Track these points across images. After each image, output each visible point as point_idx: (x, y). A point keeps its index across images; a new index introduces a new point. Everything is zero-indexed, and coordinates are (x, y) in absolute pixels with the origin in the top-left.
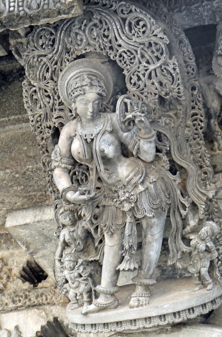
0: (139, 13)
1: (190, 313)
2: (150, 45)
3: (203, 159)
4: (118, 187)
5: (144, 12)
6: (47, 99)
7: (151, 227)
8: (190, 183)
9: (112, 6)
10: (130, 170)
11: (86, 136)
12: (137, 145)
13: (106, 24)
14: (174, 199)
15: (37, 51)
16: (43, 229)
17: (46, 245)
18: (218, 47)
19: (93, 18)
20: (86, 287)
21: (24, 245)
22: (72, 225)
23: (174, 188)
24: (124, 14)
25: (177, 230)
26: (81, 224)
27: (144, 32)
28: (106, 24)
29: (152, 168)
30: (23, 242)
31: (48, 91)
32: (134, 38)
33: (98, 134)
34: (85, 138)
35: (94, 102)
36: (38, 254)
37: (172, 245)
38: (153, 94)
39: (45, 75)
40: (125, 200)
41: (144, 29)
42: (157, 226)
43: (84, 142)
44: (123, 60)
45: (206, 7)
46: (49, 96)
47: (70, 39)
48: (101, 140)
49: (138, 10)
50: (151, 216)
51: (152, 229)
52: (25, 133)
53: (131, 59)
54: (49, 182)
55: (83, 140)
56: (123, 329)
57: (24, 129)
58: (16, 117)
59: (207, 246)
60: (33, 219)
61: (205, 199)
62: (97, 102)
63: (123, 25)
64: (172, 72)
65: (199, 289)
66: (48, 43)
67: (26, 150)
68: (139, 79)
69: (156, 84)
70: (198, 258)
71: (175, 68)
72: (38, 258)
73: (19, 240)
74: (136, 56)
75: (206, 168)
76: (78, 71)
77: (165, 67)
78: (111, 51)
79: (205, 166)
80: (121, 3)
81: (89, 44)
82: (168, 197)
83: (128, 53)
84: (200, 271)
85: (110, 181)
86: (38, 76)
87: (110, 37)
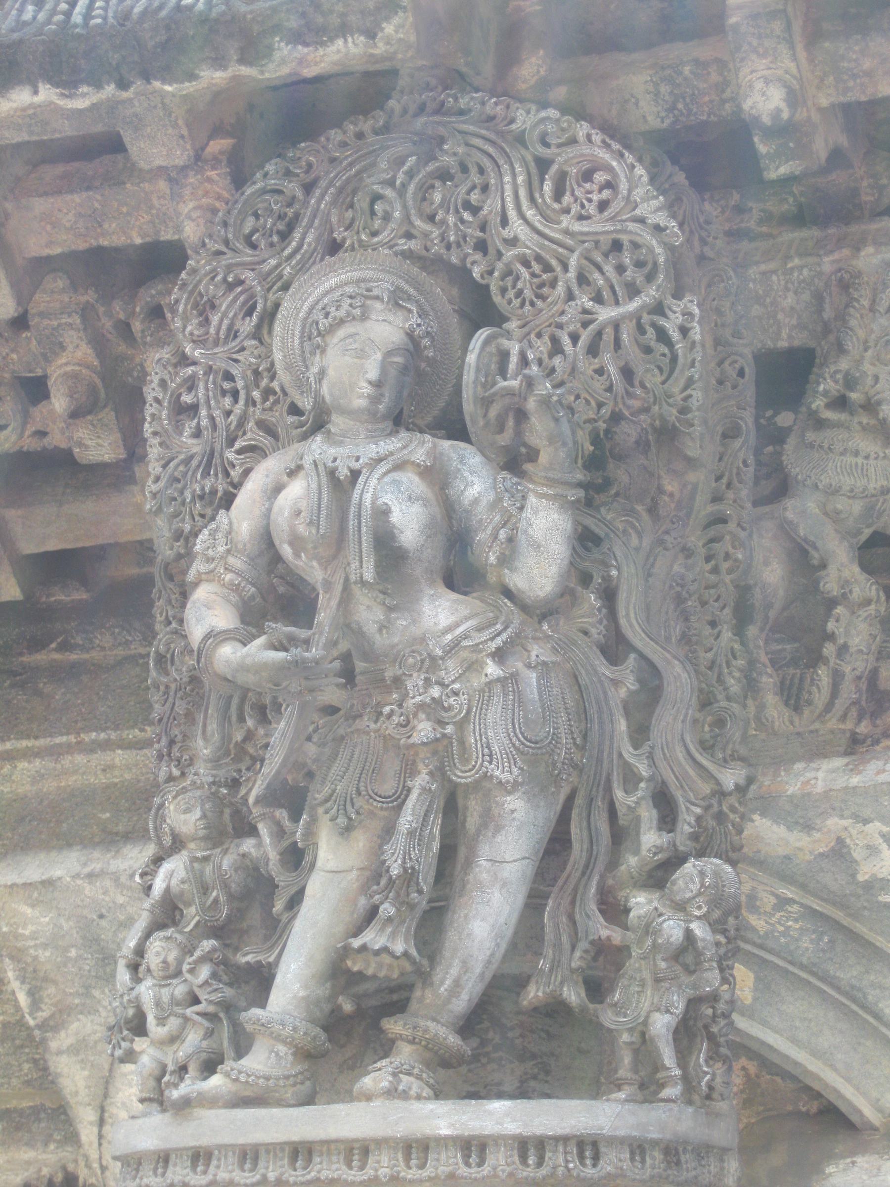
0: (599, 147)
1: (581, 1157)
2: (617, 246)
3: (720, 674)
4: (411, 660)
5: (616, 146)
6: (227, 401)
7: (498, 829)
8: (663, 723)
9: (512, 121)
10: (466, 612)
11: (335, 460)
12: (509, 526)
13: (481, 171)
14: (601, 752)
15: (230, 254)
16: (101, 916)
17: (96, 993)
18: (819, 384)
19: (441, 150)
20: (205, 1044)
21: (23, 982)
22: (205, 838)
23: (610, 708)
24: (547, 145)
25: (587, 866)
26: (238, 846)
27: (603, 206)
28: (481, 171)
29: (543, 632)
30: (24, 970)
31: (235, 372)
32: (565, 221)
33: (380, 460)
34: (330, 464)
35: (389, 354)
36: (63, 1034)
37: (557, 926)
38: (593, 403)
39: (238, 325)
40: (421, 706)
41: (606, 194)
42: (519, 828)
43: (324, 479)
44: (514, 287)
45: (796, 274)
46: (235, 394)
47: (349, 214)
48: (386, 479)
49: (597, 137)
50: (505, 777)
51: (499, 838)
52: (116, 784)
53: (541, 285)
54: (160, 720)
55: (323, 474)
56: (313, 1174)
57: (116, 773)
58: (103, 735)
59: (689, 935)
60: (76, 868)
61: (706, 788)
62: (398, 359)
63: (536, 183)
64: (675, 335)
65: (626, 1101)
66: (274, 224)
67: (108, 819)
68: (556, 348)
69: (612, 369)
70: (647, 975)
71: (689, 325)
72: (59, 1053)
73: (12, 958)
74: (561, 275)
75: (724, 704)
76: (356, 275)
77: (655, 318)
78: (478, 256)
79: (720, 697)
80: (543, 114)
81: (409, 236)
82: (578, 741)
83: (533, 263)
84: (645, 1023)
85: (380, 641)
86: (212, 331)
87: (485, 212)
